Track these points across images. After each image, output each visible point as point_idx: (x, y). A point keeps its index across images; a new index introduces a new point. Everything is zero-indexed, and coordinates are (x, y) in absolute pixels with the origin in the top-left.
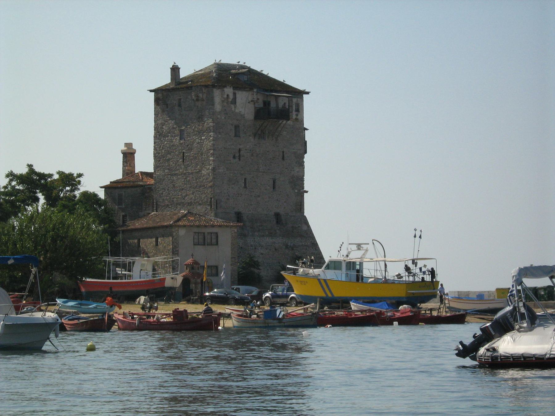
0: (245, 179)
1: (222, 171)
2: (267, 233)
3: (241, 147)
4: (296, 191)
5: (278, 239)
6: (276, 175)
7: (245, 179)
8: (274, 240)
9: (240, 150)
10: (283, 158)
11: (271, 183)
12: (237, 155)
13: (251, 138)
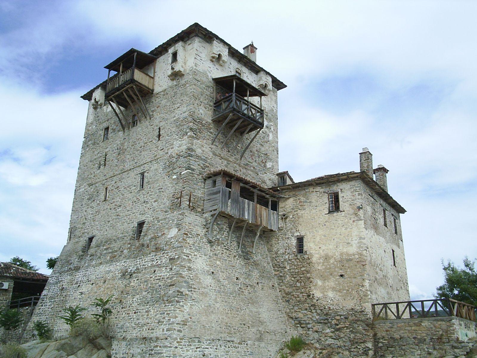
1: (83, 189)
2: (109, 257)
3: (108, 150)
4: (175, 177)
5: (118, 264)
6: (146, 165)
10: (159, 136)
12: (102, 163)
13: (119, 133)
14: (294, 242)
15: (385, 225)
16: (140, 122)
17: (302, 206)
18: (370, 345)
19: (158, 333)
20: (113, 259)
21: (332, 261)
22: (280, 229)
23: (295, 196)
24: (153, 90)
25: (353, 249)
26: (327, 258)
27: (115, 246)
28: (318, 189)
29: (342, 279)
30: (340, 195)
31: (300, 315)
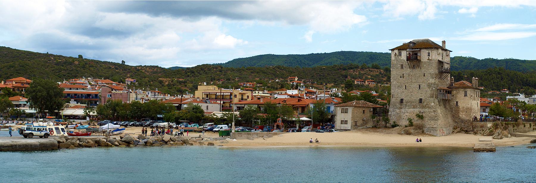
0: (406, 86)
3: (404, 73)
4: (431, 89)
7: (406, 86)
8: (415, 110)
9: (403, 74)
10: (424, 75)
11: (418, 86)
12: (402, 76)
14: (455, 103)
15: (476, 97)
16: (417, 68)
17: (458, 93)
18: (471, 127)
19: (435, 126)
20: (414, 108)
21: (464, 108)
22: (452, 99)
23: (456, 90)
24: (420, 60)
25: (469, 106)
26: (463, 107)
27: (414, 104)
28: (462, 89)
29: (466, 113)
30: (467, 92)
31: (457, 120)
